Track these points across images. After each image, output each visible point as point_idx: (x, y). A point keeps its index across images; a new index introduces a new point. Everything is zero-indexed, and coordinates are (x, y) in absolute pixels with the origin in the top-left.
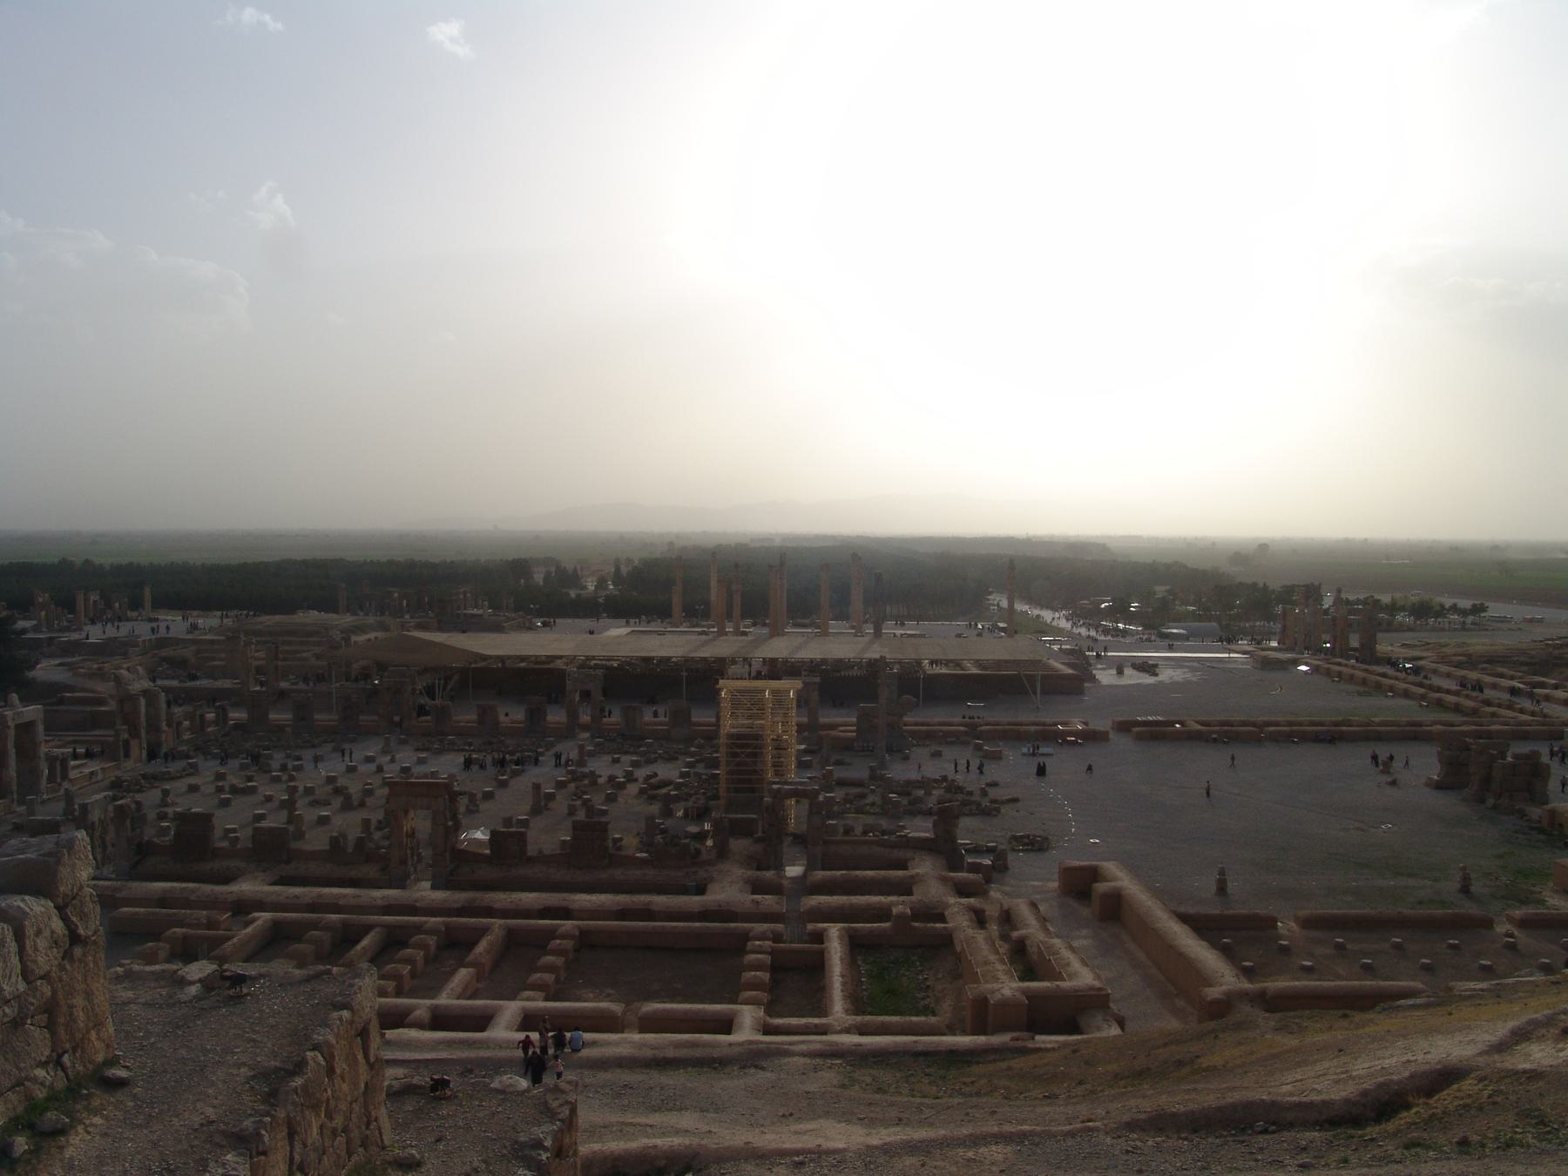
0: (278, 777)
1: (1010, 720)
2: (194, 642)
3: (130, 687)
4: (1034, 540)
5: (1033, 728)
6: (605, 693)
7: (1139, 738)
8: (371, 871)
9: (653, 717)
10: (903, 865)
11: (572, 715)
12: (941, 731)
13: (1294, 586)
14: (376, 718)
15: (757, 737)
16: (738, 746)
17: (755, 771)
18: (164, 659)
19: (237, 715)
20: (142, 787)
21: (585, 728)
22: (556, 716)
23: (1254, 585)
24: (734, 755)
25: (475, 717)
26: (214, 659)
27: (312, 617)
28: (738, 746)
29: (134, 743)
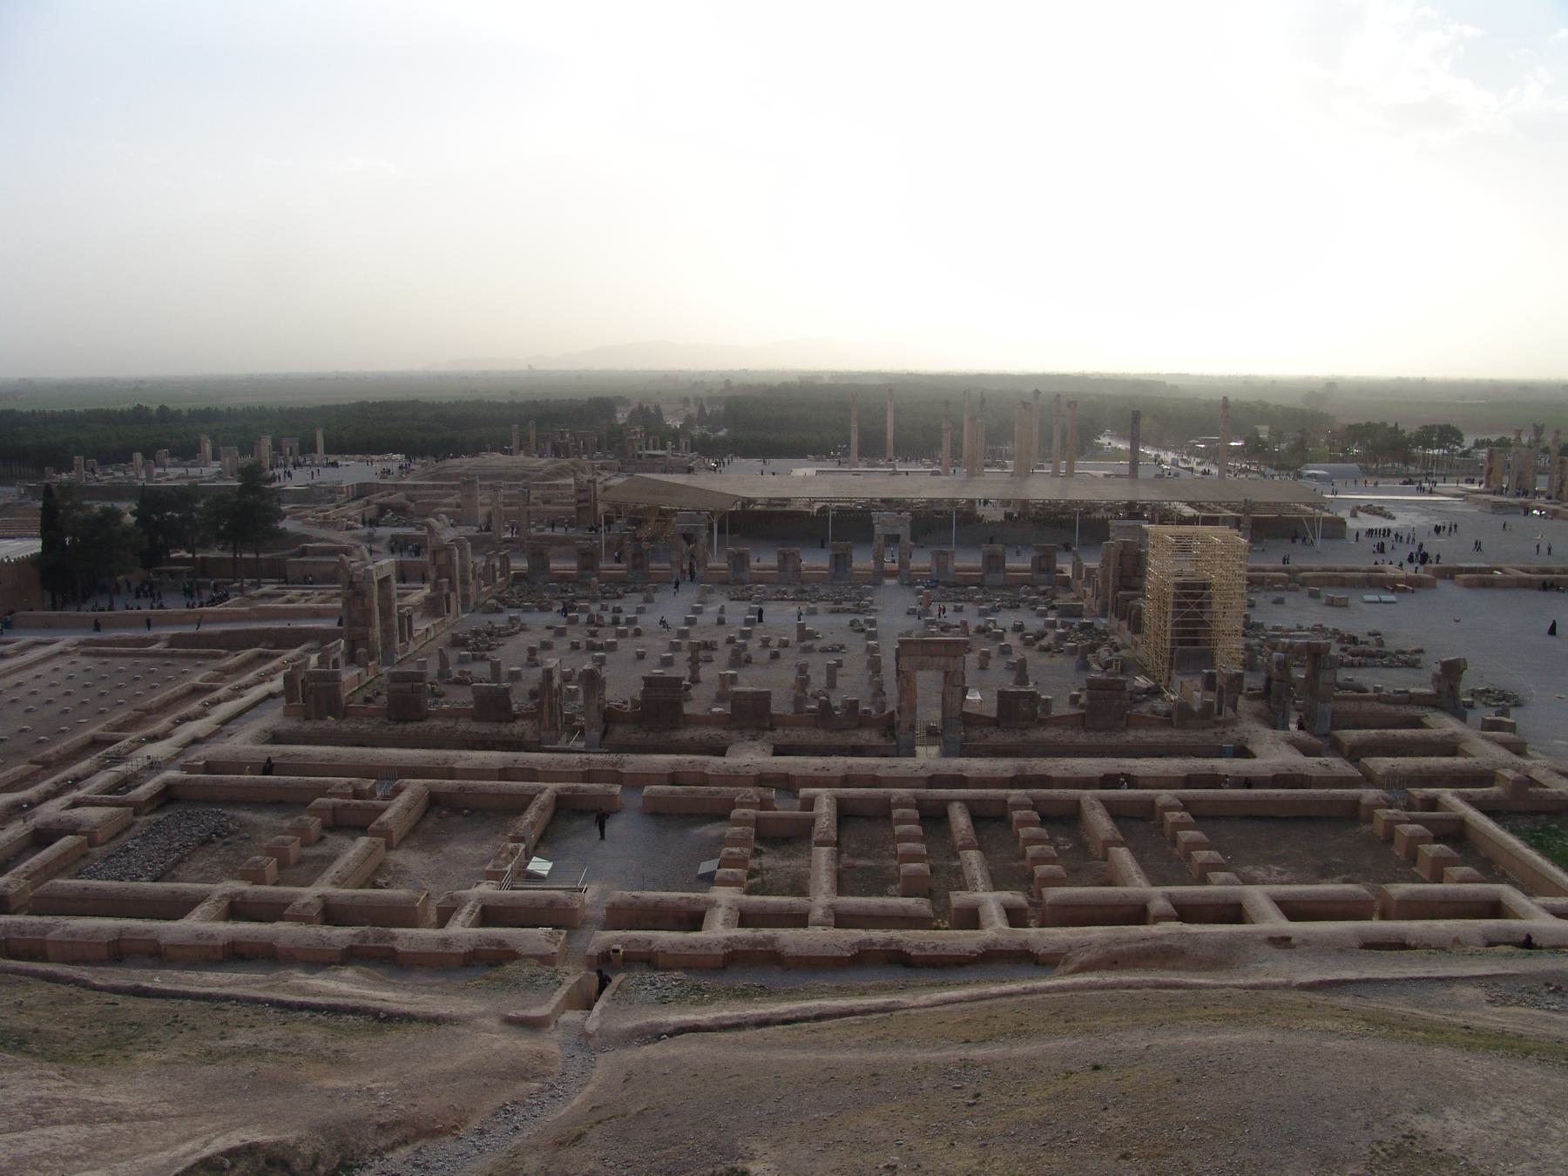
0: (626, 631)
1: (1323, 566)
2: (396, 487)
3: (443, 537)
4: (1169, 383)
5: (1360, 575)
6: (913, 538)
7: (1468, 585)
8: (867, 736)
9: (968, 560)
10: (1417, 723)
11: (879, 560)
12: (1268, 577)
13: (1434, 426)
14: (668, 565)
15: (1205, 586)
16: (1186, 596)
17: (1202, 623)
18: (382, 509)
19: (519, 564)
20: (490, 645)
21: (892, 574)
22: (862, 561)
23: (1384, 425)
24: (1186, 605)
25: (775, 563)
26: (437, 505)
27: (496, 460)
28: (1186, 596)
29: (452, 596)
